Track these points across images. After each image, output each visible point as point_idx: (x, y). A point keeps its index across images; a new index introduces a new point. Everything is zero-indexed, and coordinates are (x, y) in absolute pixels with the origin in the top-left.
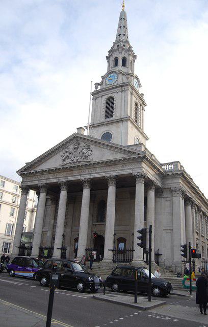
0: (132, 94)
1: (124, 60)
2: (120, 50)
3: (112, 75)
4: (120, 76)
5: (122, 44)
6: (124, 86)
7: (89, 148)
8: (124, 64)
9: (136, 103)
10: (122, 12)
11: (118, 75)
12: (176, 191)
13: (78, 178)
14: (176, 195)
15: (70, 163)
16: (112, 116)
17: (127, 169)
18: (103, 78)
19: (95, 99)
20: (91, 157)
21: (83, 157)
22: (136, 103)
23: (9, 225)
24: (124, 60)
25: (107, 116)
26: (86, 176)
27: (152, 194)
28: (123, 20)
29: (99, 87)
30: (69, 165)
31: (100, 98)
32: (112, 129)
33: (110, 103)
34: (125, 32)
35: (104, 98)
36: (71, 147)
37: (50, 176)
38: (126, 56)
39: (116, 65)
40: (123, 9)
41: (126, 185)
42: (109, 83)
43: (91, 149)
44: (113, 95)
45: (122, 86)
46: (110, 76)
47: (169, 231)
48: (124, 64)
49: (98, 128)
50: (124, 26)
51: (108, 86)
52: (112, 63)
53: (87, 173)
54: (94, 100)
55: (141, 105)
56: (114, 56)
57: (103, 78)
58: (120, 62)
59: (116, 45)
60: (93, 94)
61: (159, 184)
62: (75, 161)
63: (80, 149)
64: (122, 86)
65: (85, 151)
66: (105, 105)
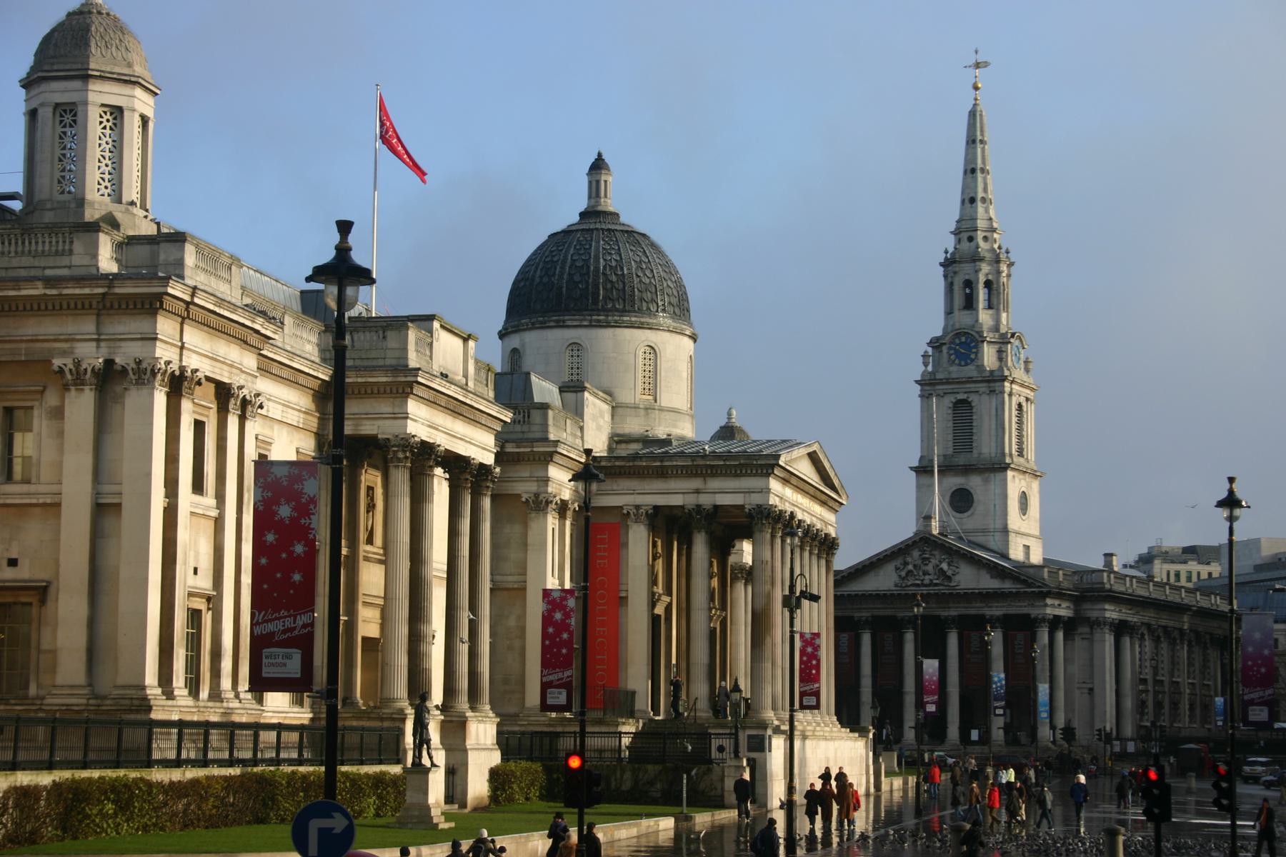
6: (995, 381)
9: (1020, 405)
11: (976, 347)
15: (918, 585)
19: (925, 396)
20: (957, 578)
22: (1020, 405)
27: (1060, 635)
32: (974, 483)
33: (962, 410)
34: (985, 190)
35: (949, 401)
36: (916, 553)
39: (970, 303)
41: (1021, 629)
44: (972, 398)
59: (965, 236)
65: (944, 566)
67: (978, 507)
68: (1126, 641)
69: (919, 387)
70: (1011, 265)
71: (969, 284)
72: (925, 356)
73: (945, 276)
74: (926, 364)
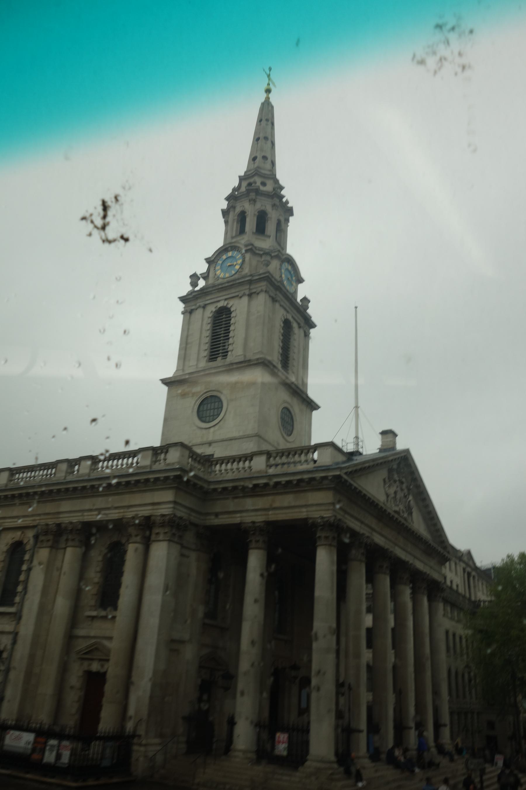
0: (274, 300)
1: (262, 219)
2: (253, 195)
3: (230, 254)
4: (248, 256)
5: (258, 181)
8: (261, 229)
9: (287, 324)
10: (263, 104)
16: (225, 355)
18: (210, 261)
19: (188, 313)
24: (262, 219)
25: (213, 356)
28: (264, 122)
29: (202, 283)
31: (200, 311)
38: (269, 209)
39: (242, 231)
40: (268, 99)
42: (222, 274)
45: (250, 282)
46: (224, 257)
48: (261, 229)
50: (266, 138)
51: (220, 281)
52: (236, 226)
54: (188, 315)
55: (300, 327)
56: (238, 210)
57: (210, 261)
58: (251, 224)
59: (244, 184)
60: (183, 299)
64: (250, 282)
66: (209, 327)
71: (242, 217)
72: (194, 278)
73: (226, 222)
74: (194, 284)
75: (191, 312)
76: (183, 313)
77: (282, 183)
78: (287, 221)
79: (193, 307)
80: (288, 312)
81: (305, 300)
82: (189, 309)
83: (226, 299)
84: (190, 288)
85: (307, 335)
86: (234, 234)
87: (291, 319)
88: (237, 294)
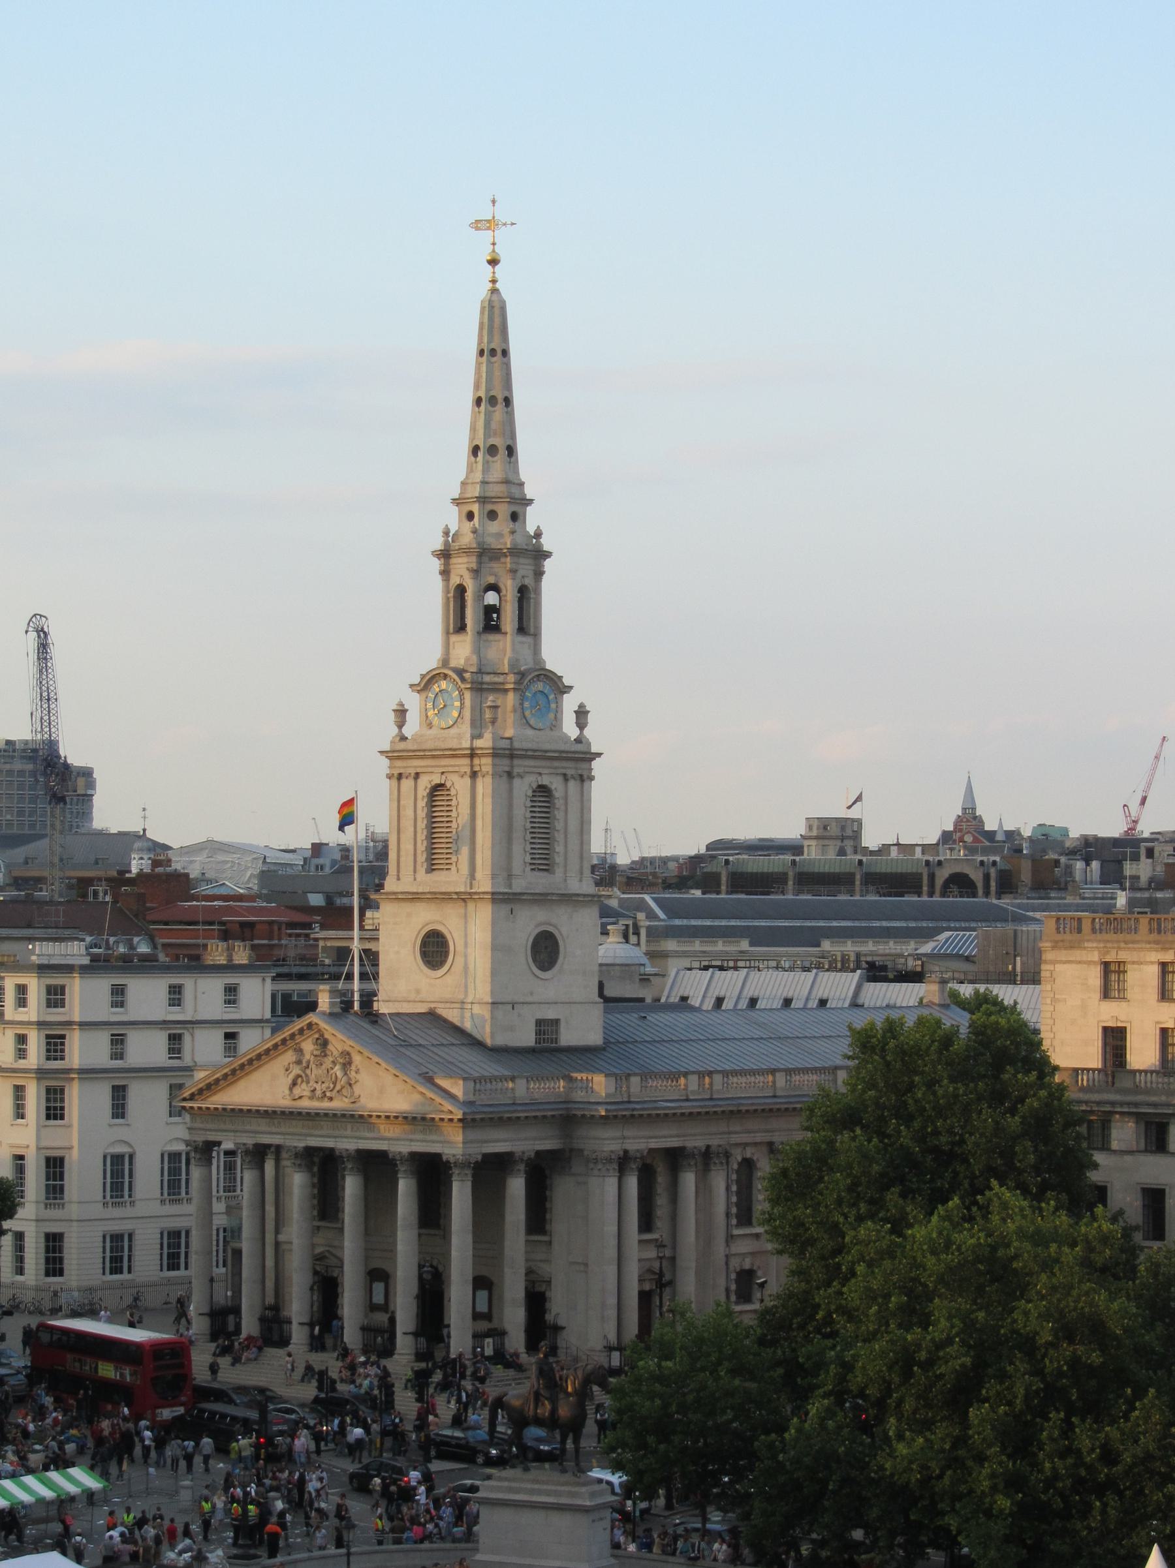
7: (350, 1063)
12: (596, 1161)
13: (329, 1143)
14: (596, 1172)
17: (433, 1142)
21: (338, 1087)
22: (543, 791)
23: (174, 1157)
26: (347, 1142)
30: (306, 1104)
35: (425, 783)
37: (263, 1125)
43: (353, 1068)
47: (582, 1268)
49: (407, 907)
53: (349, 1132)
55: (566, 778)
61: (549, 1144)
62: (318, 1093)
63: (328, 1062)
67: (455, 961)
68: (689, 1180)
69: (386, 762)
70: (547, 555)
74: (401, 724)
75: (400, 777)
76: (390, 777)
77: (529, 492)
78: (539, 574)
79: (401, 771)
80: (540, 774)
81: (582, 715)
82: (396, 772)
83: (443, 773)
84: (395, 730)
85: (585, 778)
86: (451, 630)
87: (545, 781)
88: (456, 769)
